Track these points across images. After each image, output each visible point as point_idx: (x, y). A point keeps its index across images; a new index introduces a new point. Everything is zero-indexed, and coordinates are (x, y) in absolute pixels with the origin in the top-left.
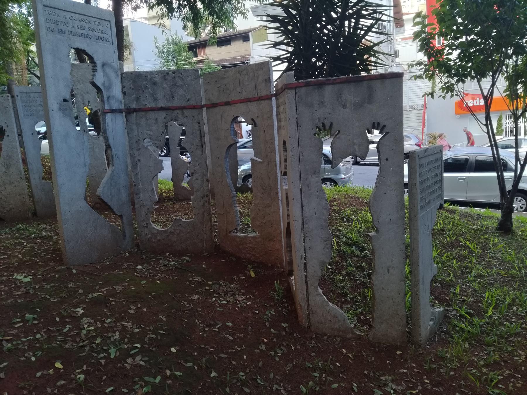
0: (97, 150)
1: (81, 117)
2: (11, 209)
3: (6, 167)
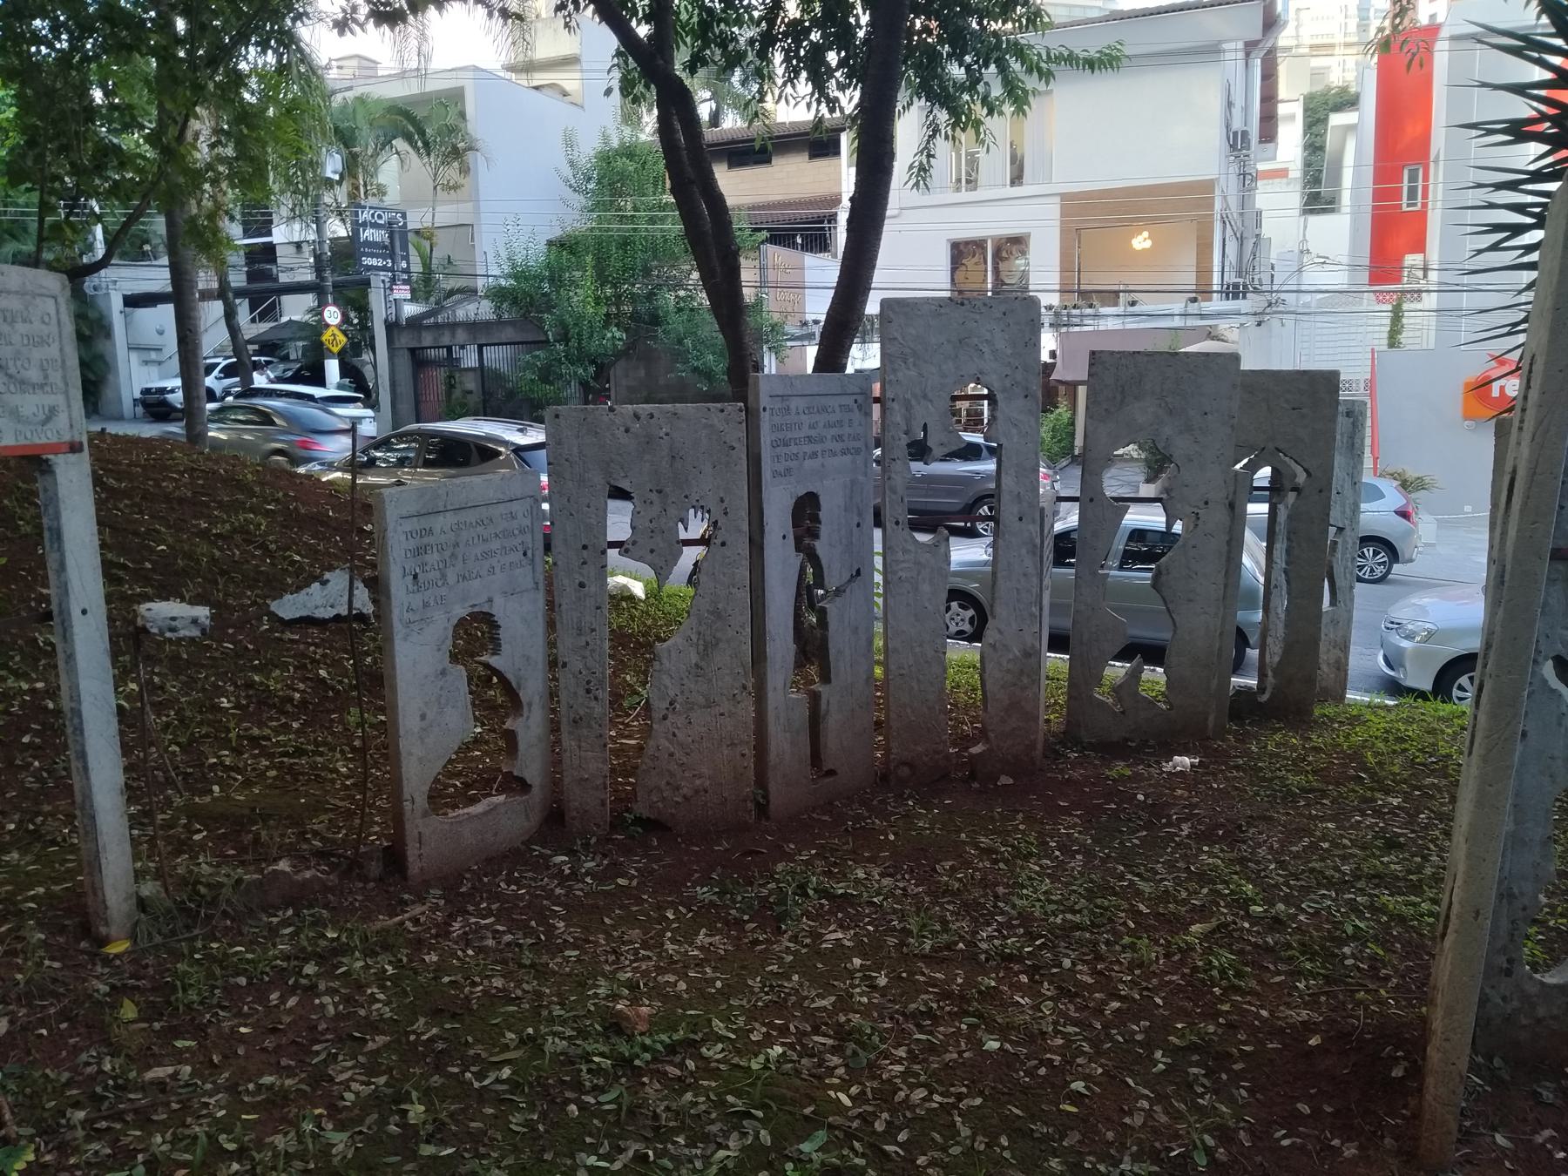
0: (926, 588)
1: (893, 475)
2: (697, 792)
3: (701, 648)
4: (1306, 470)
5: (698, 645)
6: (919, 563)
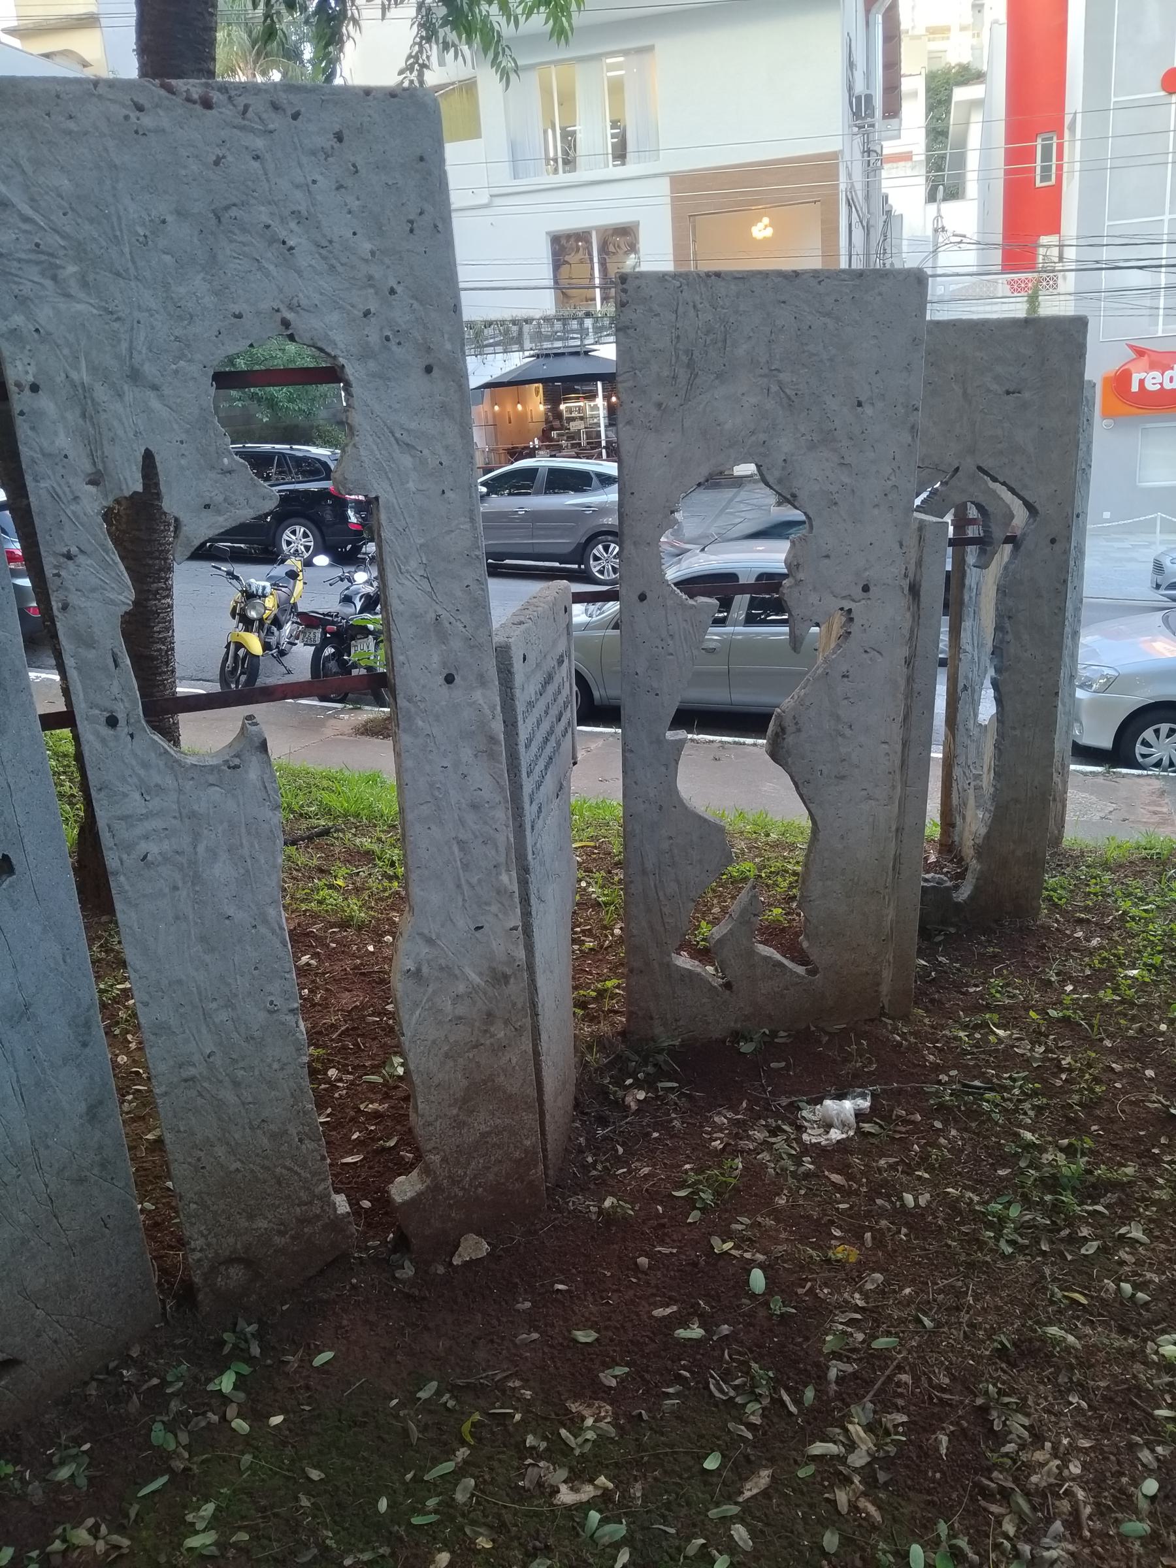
0: (221, 871)
1: (74, 599)
4: (1029, 506)
6: (193, 815)
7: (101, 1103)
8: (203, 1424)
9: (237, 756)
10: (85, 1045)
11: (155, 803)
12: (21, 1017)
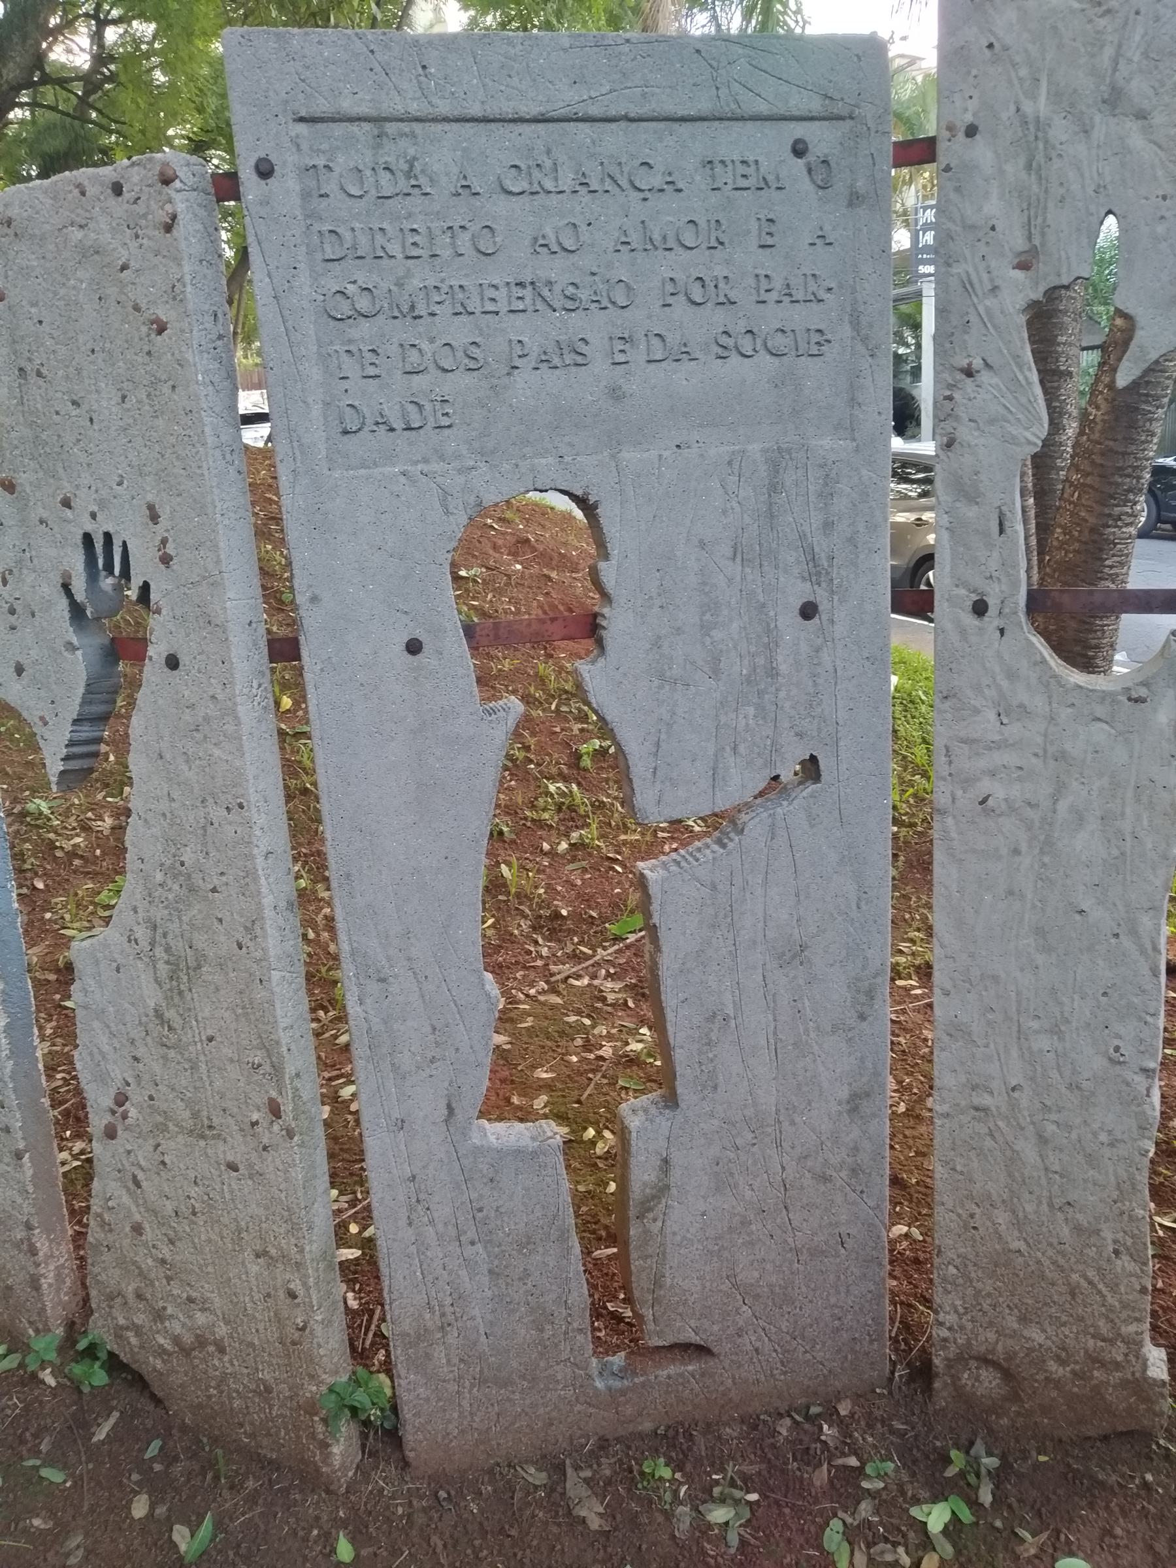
1: (965, 433)
2: (201, 1342)
3: (163, 969)
5: (153, 961)
6: (1062, 756)
7: (868, 1095)
8: (889, 1558)
9: (1145, 684)
10: (862, 1017)
11: (1014, 730)
12: (794, 957)
